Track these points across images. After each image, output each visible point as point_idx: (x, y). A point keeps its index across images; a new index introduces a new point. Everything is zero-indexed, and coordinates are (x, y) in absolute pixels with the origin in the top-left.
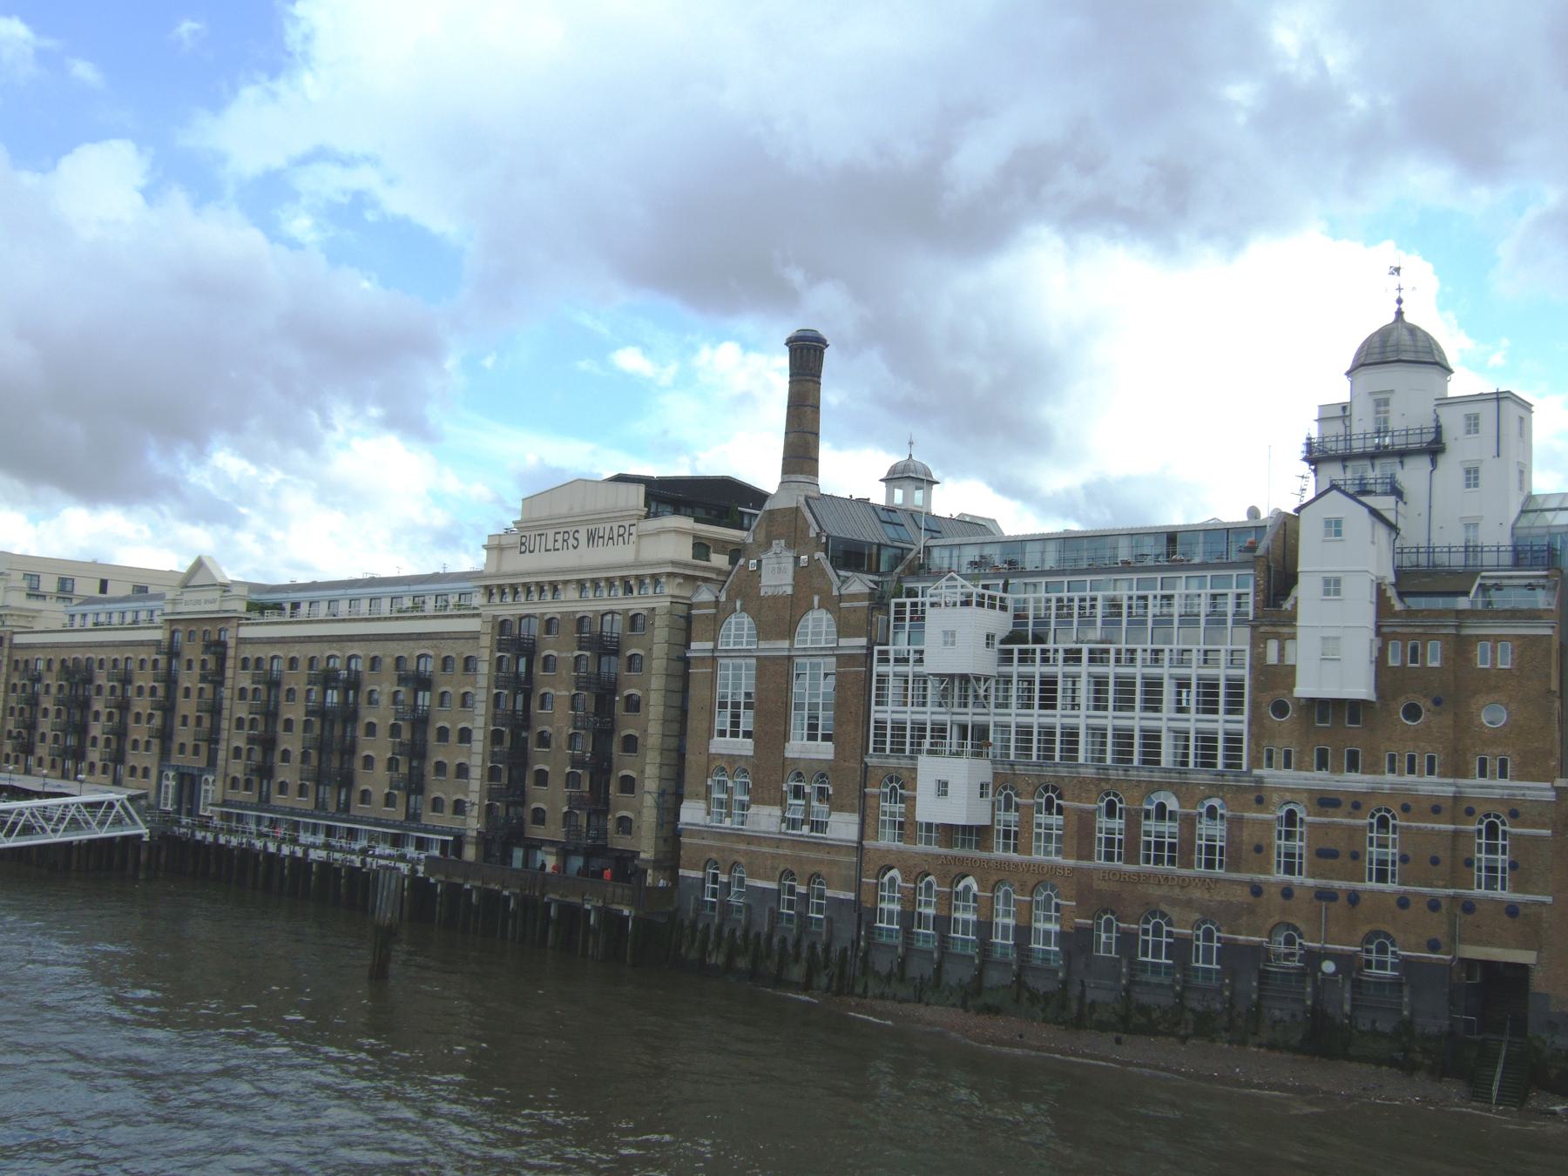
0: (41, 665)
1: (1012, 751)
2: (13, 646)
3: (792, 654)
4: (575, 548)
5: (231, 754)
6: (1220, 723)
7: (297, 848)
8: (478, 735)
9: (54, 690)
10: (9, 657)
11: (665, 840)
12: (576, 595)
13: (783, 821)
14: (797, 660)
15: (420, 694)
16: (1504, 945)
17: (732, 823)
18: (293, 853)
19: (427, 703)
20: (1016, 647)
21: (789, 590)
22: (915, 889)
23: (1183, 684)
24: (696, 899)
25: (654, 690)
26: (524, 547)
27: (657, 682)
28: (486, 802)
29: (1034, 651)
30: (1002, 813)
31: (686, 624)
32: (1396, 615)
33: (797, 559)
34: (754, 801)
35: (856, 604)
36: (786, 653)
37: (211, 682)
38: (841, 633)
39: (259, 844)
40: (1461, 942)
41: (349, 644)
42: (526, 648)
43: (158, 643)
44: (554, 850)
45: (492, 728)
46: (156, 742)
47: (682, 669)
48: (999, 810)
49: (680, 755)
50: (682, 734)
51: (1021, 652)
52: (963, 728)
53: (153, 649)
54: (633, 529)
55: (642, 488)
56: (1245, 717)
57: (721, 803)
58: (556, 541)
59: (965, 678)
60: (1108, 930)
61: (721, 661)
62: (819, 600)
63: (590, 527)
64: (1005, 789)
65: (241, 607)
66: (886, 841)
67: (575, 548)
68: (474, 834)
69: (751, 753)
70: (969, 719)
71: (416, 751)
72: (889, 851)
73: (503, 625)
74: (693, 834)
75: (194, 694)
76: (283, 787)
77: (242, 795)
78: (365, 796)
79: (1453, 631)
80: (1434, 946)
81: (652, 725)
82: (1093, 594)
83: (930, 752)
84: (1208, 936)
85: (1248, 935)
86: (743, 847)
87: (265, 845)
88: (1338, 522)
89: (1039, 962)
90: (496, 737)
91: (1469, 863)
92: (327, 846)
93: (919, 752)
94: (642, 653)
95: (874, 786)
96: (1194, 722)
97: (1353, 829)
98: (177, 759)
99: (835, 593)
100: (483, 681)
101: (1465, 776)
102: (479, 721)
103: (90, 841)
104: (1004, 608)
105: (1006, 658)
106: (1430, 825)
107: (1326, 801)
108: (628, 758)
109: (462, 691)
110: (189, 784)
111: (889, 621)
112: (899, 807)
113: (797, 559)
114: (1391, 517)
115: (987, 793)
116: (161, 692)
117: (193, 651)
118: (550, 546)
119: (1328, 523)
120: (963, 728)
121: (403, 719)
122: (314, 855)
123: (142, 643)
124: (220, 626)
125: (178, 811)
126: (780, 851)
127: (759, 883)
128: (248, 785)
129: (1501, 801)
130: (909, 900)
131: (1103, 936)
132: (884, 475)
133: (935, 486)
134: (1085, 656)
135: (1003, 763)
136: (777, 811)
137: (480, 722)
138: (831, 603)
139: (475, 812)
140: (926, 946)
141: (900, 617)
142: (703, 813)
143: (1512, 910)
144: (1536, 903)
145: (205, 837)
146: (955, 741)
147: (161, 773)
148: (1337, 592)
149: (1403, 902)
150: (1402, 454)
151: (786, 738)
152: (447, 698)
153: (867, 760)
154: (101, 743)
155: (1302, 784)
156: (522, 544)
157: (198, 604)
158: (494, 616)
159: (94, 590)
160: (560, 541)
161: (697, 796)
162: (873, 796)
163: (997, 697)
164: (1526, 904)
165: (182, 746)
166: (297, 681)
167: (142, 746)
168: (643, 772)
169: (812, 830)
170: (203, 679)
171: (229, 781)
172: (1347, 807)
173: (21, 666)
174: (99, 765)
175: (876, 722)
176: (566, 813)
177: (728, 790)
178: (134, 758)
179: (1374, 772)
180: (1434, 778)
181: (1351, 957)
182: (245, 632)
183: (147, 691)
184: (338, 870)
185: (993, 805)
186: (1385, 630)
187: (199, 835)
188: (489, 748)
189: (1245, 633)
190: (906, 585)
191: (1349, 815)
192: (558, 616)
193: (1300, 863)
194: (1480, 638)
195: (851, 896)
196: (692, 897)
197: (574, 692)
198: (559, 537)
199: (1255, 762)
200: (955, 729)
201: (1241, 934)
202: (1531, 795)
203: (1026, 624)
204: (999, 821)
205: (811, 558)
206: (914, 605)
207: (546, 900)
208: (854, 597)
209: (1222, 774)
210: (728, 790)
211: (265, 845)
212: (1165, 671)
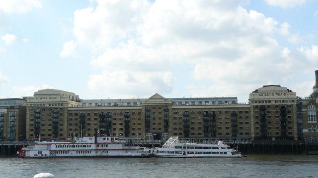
73: (257, 107)
182: (173, 107)
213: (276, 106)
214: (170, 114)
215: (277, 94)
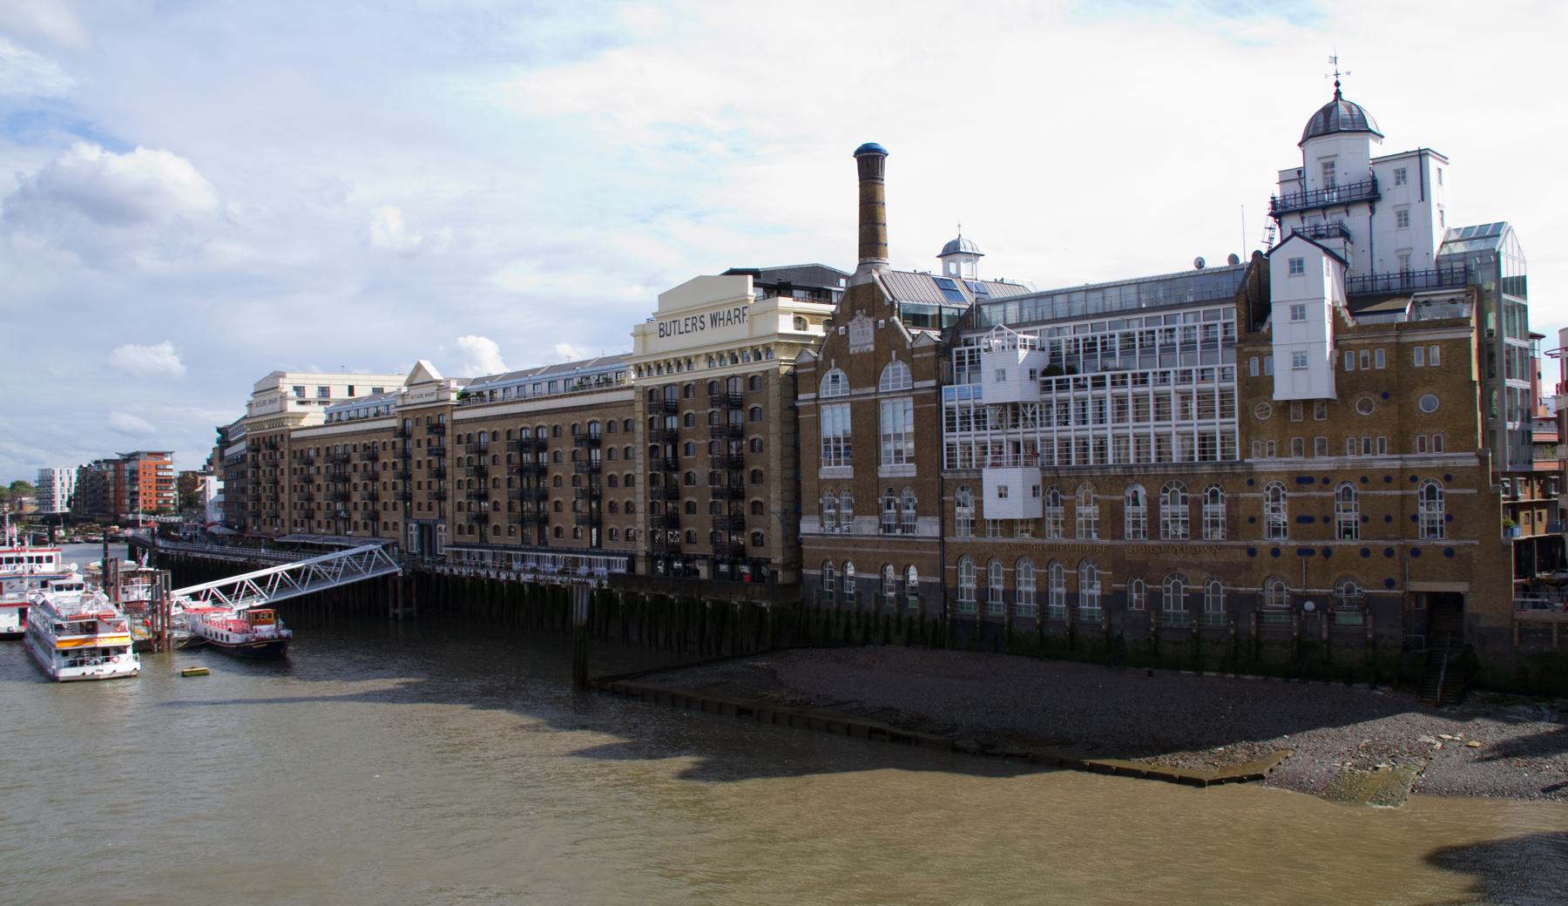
0: (312, 453)
1: (1056, 460)
2: (292, 441)
3: (879, 397)
4: (702, 329)
5: (456, 508)
6: (1216, 425)
7: (511, 574)
8: (640, 479)
9: (323, 470)
10: (289, 449)
11: (790, 547)
12: (706, 366)
13: (880, 527)
14: (883, 402)
15: (593, 451)
16: (1444, 579)
17: (841, 531)
18: (509, 577)
19: (599, 457)
20: (1053, 378)
21: (872, 348)
22: (986, 571)
23: (1186, 397)
24: (818, 591)
25: (771, 434)
26: (663, 332)
27: (774, 428)
28: (651, 529)
29: (1068, 380)
30: (1208, 506)
31: (793, 382)
32: (1349, 331)
33: (876, 323)
34: (855, 513)
35: (925, 355)
36: (873, 397)
37: (437, 455)
38: (915, 379)
39: (483, 573)
40: (1411, 578)
41: (536, 418)
42: (672, 410)
43: (394, 428)
44: (705, 562)
45: (650, 473)
46: (400, 504)
47: (792, 415)
48: (1049, 505)
49: (797, 481)
50: (797, 465)
51: (1057, 381)
52: (1017, 445)
53: (391, 434)
54: (745, 310)
55: (750, 278)
56: (1236, 419)
57: (831, 517)
58: (687, 325)
59: (1015, 406)
60: (1139, 590)
61: (823, 407)
62: (897, 354)
63: (712, 312)
64: (1052, 488)
65: (454, 397)
66: (963, 535)
67: (702, 329)
68: (644, 554)
69: (852, 476)
70: (1020, 437)
71: (593, 495)
72: (965, 544)
73: (650, 393)
74: (811, 543)
75: (424, 465)
76: (497, 530)
77: (467, 538)
78: (558, 531)
79: (1394, 340)
80: (1390, 584)
81: (773, 461)
82: (1112, 332)
83: (993, 465)
84: (1216, 589)
85: (1247, 587)
86: (851, 549)
87: (488, 573)
88: (1300, 262)
89: (1086, 619)
90: (653, 480)
91: (1415, 518)
92: (534, 570)
93: (983, 465)
94: (760, 406)
95: (949, 495)
96: (1196, 426)
97: (1322, 498)
98: (416, 514)
99: (908, 347)
100: (640, 439)
101: (1409, 453)
102: (639, 468)
103: (360, 582)
104: (1042, 349)
105: (1046, 387)
106: (1383, 492)
107: (1303, 480)
108: (755, 487)
109: (624, 446)
110: (427, 531)
111: (952, 366)
112: (1060, 509)
113: (876, 323)
114: (1341, 254)
115: (1038, 494)
116: (400, 466)
117: (421, 433)
118: (682, 329)
119: (1292, 262)
120: (1017, 445)
121: (582, 472)
122: (526, 577)
123: (383, 430)
124: (438, 413)
125: (422, 553)
126: (880, 550)
127: (865, 576)
128: (471, 531)
129: (1438, 469)
130: (983, 579)
131: (1135, 596)
132: (940, 253)
133: (981, 258)
134: (1108, 381)
135: (1049, 469)
136: (875, 519)
137: (640, 469)
138: (907, 354)
139: (642, 538)
140: (998, 613)
141: (961, 362)
142: (818, 525)
143: (1449, 552)
144: (1466, 545)
145: (443, 571)
146: (1010, 455)
147: (406, 525)
148: (1303, 316)
149: (1365, 552)
150: (1346, 205)
151: (878, 462)
152: (613, 452)
153: (943, 474)
154: (361, 507)
155: (1283, 468)
156: (661, 330)
157: (423, 396)
158: (644, 387)
159: (345, 395)
160: (690, 325)
161: (812, 513)
162: (948, 502)
163: (1041, 419)
164: (1459, 547)
165: (420, 504)
166: (500, 449)
167: (390, 507)
168: (769, 497)
169: (903, 532)
170: (430, 452)
171: (456, 527)
172: (1318, 483)
173: (298, 455)
174: (361, 523)
175: (948, 445)
176: (712, 534)
177: (836, 507)
178: (384, 517)
179: (1339, 454)
180: (1385, 456)
181: (1327, 597)
182: (458, 415)
183: (390, 466)
184: (542, 588)
185: (1044, 502)
186: (1340, 343)
187: (439, 569)
188: (649, 489)
189: (1233, 353)
190: (963, 337)
191: (1321, 489)
192: (693, 383)
193: (1356, 529)
194: (1415, 344)
195: (938, 580)
196: (814, 591)
197: (710, 440)
198: (689, 322)
199: (1246, 453)
200: (1010, 445)
201: (1241, 586)
202: (1461, 463)
203: (1061, 360)
204: (1049, 514)
205: (887, 321)
206: (971, 351)
207: (702, 599)
208: (923, 349)
209: (1221, 465)
210: (836, 507)
211: (488, 573)
212: (1172, 388)
213: (711, 385)
214: (448, 441)
215: (714, 320)
